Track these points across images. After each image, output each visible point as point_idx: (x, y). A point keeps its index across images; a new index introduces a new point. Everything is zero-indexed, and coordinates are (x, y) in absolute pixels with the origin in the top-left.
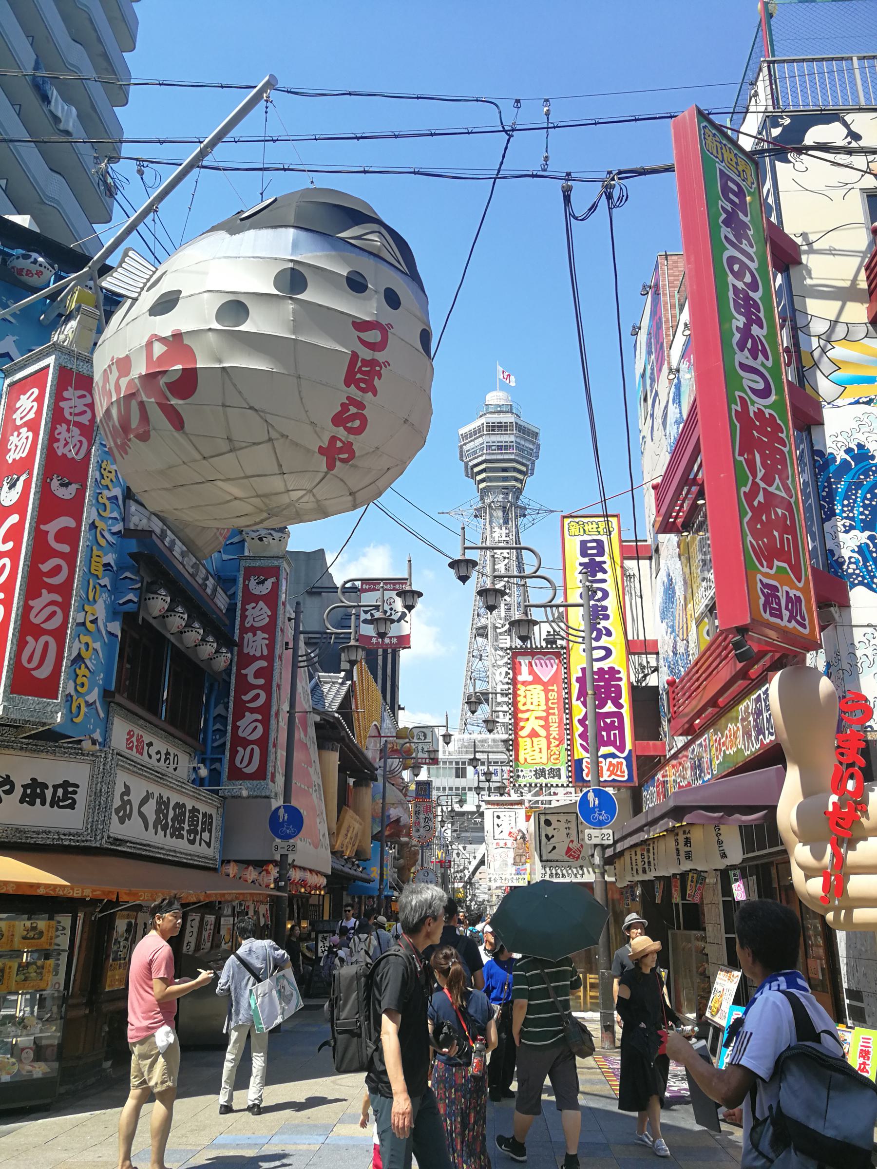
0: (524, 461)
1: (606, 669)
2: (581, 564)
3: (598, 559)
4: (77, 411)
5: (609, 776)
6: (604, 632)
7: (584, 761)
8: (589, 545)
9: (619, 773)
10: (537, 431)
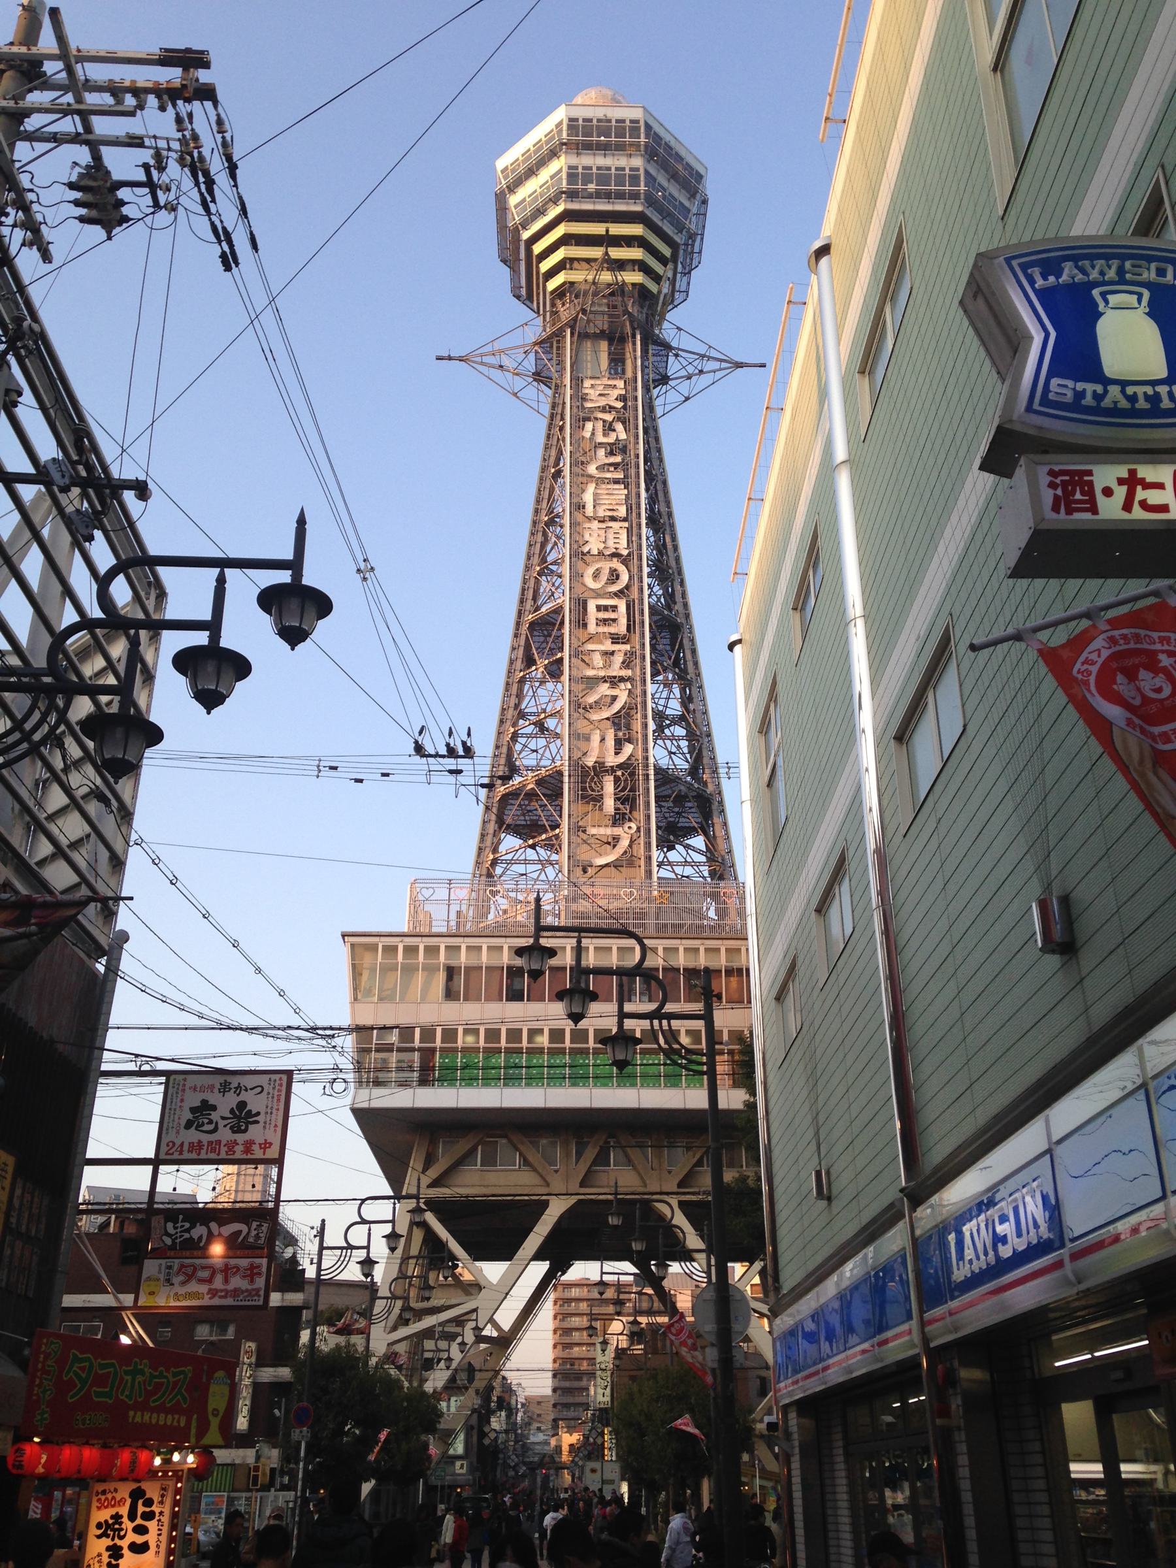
0: (668, 229)
10: (702, 171)
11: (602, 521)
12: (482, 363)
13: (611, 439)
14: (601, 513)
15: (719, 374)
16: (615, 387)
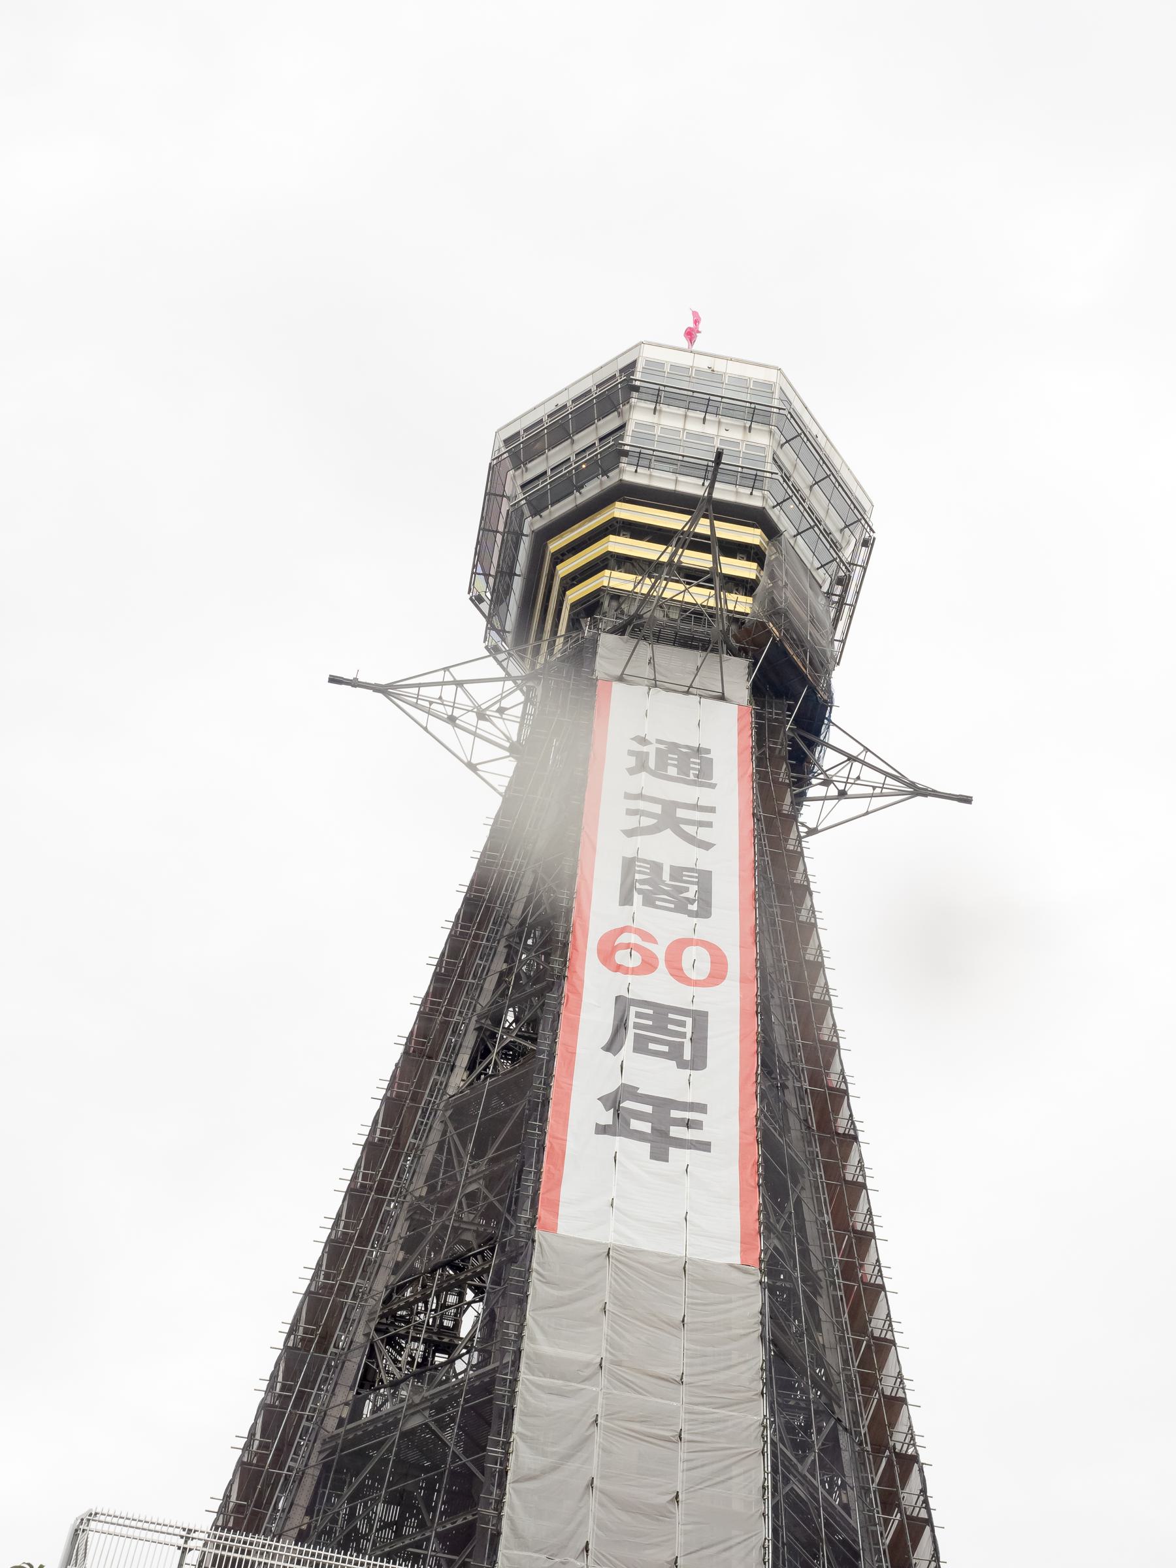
12: (416, 706)
15: (878, 802)
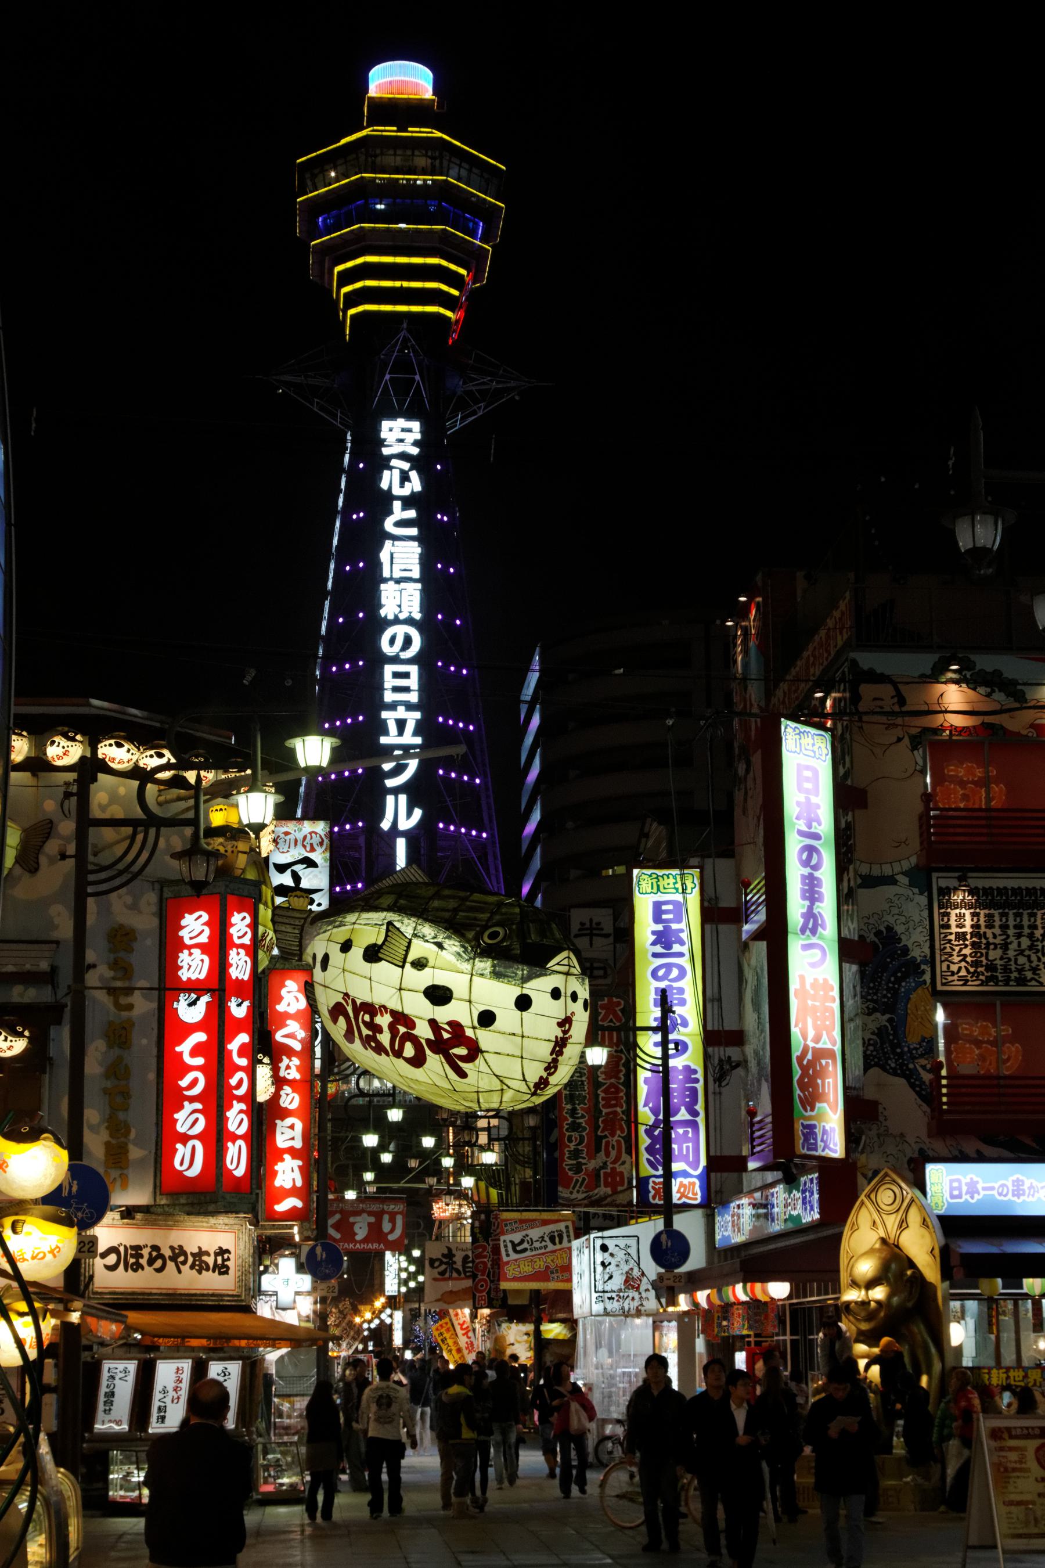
1: (680, 1068)
2: (654, 933)
3: (674, 926)
4: (241, 934)
5: (679, 1199)
6: (679, 1022)
7: (651, 1180)
8: (664, 907)
9: (690, 1195)
11: (398, 581)
13: (406, 491)
14: (397, 575)
16: (410, 430)
